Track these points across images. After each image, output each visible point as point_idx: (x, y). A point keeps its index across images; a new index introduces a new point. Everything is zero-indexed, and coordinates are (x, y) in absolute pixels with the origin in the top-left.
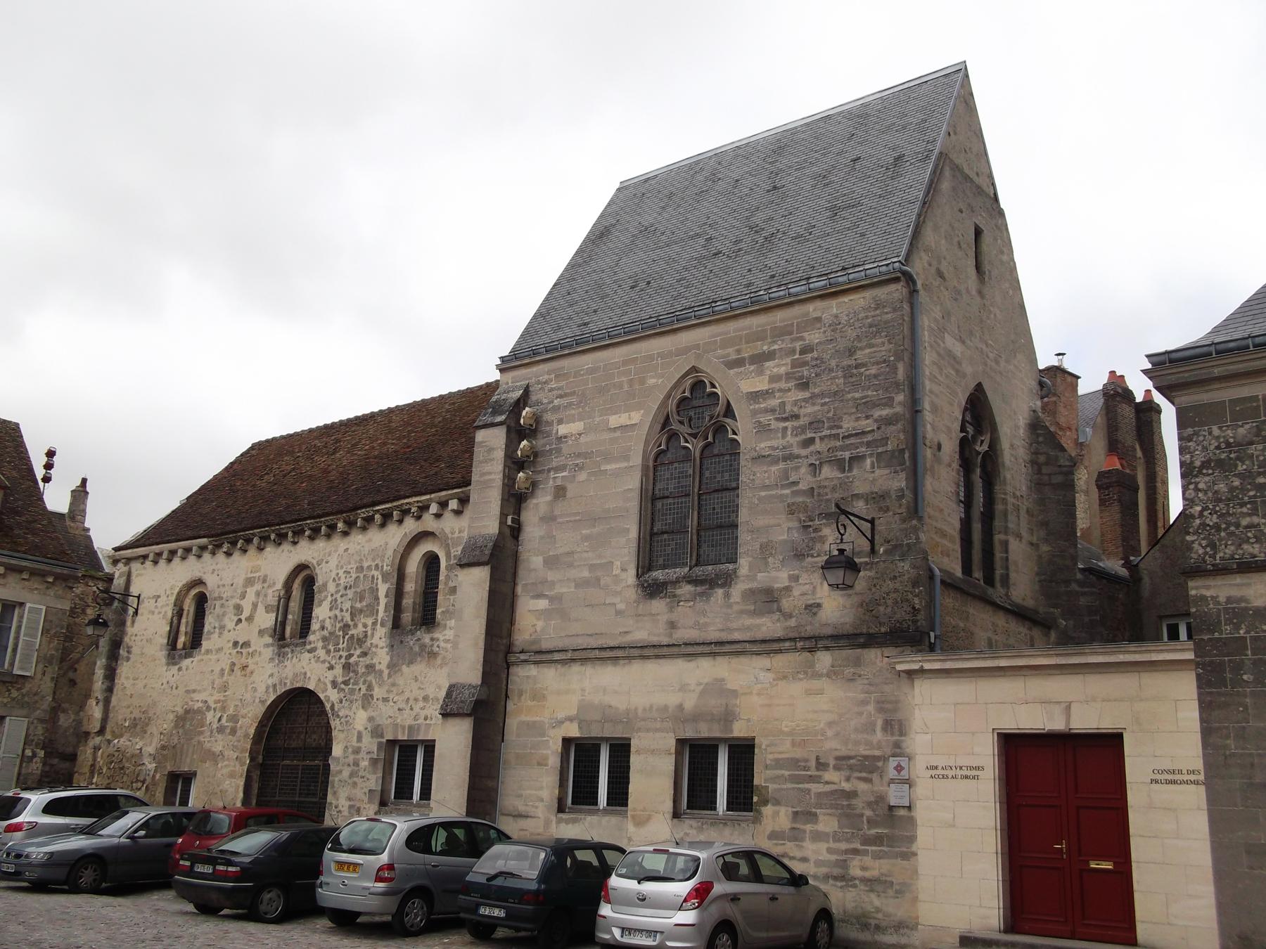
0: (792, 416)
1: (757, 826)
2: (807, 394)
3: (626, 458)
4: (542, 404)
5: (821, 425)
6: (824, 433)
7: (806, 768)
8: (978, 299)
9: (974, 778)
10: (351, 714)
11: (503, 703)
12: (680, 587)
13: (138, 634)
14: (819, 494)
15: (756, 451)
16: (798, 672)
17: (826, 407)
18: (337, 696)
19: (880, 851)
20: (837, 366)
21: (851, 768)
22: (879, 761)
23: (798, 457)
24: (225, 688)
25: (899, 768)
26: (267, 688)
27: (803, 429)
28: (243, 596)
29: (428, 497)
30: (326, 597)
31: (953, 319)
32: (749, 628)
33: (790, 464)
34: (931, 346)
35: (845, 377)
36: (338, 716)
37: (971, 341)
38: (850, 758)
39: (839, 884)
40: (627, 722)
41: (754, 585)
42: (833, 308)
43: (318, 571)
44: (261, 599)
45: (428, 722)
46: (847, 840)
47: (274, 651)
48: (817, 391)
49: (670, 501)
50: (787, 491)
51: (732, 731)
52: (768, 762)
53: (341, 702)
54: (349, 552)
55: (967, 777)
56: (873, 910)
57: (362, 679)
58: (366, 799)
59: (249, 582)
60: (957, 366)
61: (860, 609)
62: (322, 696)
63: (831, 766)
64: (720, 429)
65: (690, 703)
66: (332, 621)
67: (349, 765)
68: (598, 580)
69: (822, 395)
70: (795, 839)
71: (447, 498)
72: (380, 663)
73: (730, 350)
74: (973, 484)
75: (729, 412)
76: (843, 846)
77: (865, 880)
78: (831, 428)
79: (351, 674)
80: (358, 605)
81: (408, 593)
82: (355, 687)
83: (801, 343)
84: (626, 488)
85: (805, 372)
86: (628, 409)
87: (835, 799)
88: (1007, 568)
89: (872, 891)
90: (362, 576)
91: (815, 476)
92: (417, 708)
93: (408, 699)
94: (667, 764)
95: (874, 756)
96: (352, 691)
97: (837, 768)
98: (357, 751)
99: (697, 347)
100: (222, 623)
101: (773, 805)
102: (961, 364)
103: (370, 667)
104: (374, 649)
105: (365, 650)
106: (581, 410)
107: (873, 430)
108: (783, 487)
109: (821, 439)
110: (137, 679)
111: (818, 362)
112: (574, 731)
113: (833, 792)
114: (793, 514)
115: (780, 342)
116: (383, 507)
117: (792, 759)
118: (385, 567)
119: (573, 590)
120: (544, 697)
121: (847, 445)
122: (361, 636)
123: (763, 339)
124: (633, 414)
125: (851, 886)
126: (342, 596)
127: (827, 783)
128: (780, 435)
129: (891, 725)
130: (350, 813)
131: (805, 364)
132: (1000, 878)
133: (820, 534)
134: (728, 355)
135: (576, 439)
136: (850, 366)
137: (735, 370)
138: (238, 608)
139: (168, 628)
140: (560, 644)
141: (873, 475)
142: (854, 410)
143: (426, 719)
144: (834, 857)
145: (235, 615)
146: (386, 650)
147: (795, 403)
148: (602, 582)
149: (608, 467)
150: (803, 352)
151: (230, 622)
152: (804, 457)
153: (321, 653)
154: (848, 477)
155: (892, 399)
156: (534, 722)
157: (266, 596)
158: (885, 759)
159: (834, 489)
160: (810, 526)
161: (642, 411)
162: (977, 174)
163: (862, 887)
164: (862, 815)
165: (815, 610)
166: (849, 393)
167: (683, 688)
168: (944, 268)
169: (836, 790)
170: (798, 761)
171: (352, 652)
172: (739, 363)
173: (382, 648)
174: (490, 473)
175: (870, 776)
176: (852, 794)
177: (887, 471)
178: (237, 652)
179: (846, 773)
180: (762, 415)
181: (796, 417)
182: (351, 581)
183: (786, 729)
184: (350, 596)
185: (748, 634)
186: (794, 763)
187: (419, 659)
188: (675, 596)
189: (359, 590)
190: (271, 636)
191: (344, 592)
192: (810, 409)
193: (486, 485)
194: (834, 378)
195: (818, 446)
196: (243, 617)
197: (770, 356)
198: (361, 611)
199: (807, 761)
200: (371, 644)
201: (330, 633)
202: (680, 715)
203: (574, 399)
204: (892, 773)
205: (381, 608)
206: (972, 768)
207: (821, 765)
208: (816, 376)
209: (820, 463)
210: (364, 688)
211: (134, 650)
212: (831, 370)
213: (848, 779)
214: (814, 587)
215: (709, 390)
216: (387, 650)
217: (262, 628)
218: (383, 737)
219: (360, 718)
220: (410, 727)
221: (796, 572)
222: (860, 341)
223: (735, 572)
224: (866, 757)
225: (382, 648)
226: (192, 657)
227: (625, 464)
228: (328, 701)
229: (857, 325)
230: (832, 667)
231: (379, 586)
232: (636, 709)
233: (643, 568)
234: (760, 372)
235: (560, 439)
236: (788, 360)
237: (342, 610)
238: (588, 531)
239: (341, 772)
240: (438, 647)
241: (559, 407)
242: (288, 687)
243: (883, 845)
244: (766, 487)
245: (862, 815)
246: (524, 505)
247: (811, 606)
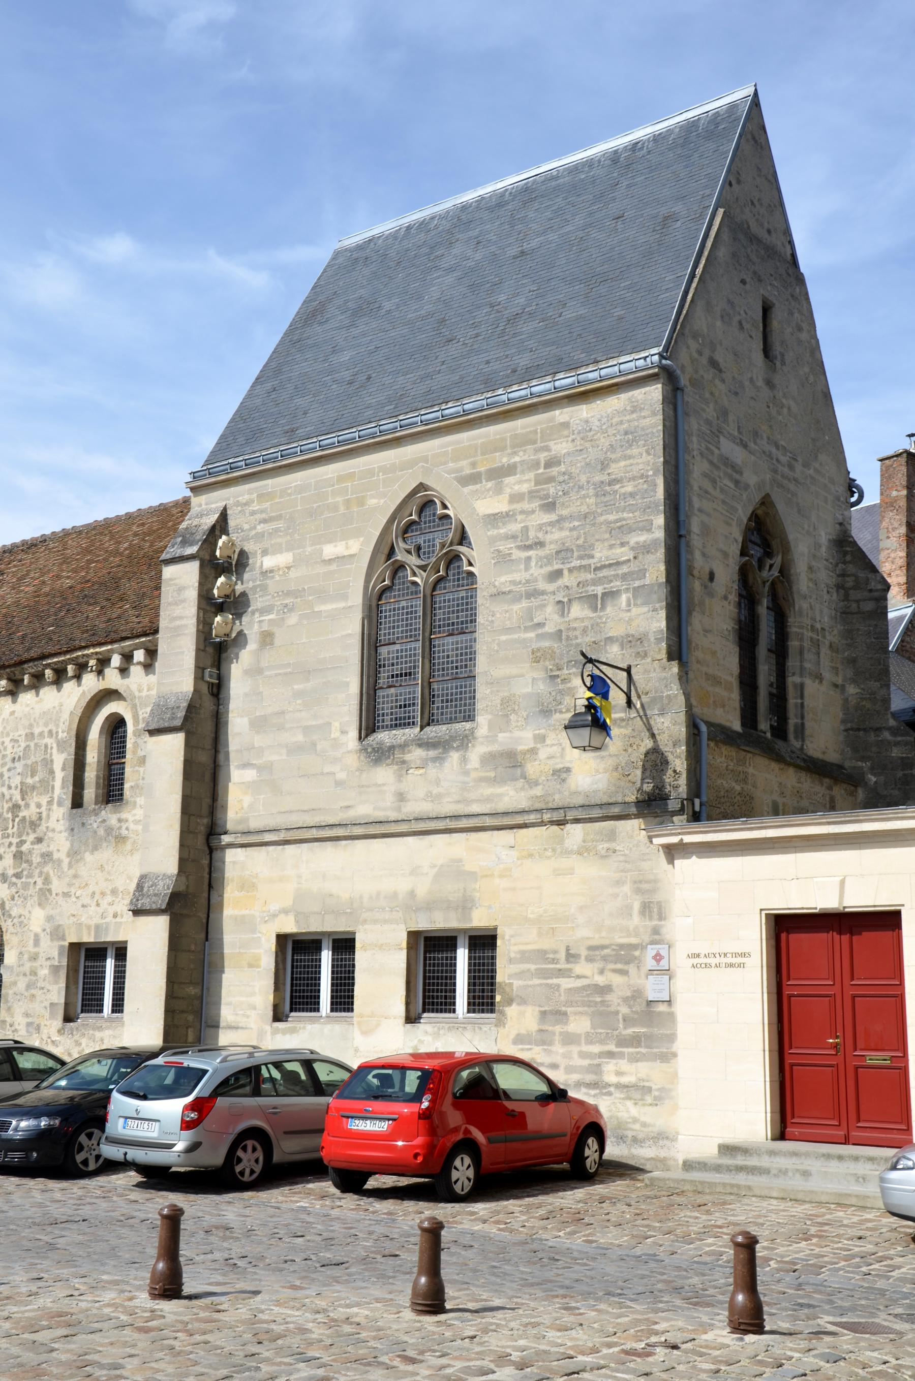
0: (536, 544)
1: (501, 1030)
2: (553, 517)
3: (344, 597)
4: (242, 531)
5: (569, 555)
6: (573, 565)
7: (554, 961)
8: (766, 392)
9: (739, 966)
10: (26, 913)
11: (205, 895)
12: (409, 752)
14: (568, 638)
15: (495, 587)
16: (545, 849)
17: (575, 533)
18: (8, 892)
19: (637, 1053)
20: (588, 482)
21: (605, 959)
22: (636, 950)
23: (543, 593)
25: (658, 958)
27: (549, 559)
29: (109, 647)
31: (731, 418)
32: (488, 799)
33: (535, 602)
34: (701, 454)
35: (597, 495)
36: (10, 916)
37: (755, 443)
38: (603, 947)
40: (351, 913)
41: (495, 748)
42: (584, 411)
45: (118, 919)
46: (602, 1042)
48: (565, 512)
49: (397, 647)
50: (532, 635)
51: (471, 920)
52: (512, 955)
53: (13, 899)
54: (16, 715)
55: (731, 965)
56: (629, 1120)
57: (38, 871)
58: (47, 1015)
60: (737, 477)
61: (615, 774)
63: (583, 958)
64: (453, 559)
65: (423, 888)
67: (25, 975)
68: (314, 744)
69: (571, 517)
70: (543, 1043)
71: (131, 648)
73: (464, 463)
74: (758, 617)
75: (463, 538)
76: (596, 1049)
77: (618, 1086)
78: (581, 558)
79: (24, 865)
80: (29, 781)
81: (90, 765)
82: (28, 880)
83: (546, 454)
84: (344, 633)
85: (552, 489)
86: (345, 536)
87: (588, 995)
88: (803, 717)
90: (32, 744)
91: (563, 615)
92: (104, 903)
93: (94, 893)
94: (398, 960)
96: (26, 886)
97: (590, 959)
98: (34, 958)
99: (425, 459)
101: (519, 1004)
102: (741, 473)
103: (47, 856)
104: (50, 834)
105: (41, 835)
106: (289, 537)
107: (629, 561)
108: (526, 629)
109: (570, 570)
111: (566, 477)
112: (290, 927)
113: (584, 988)
114: (539, 662)
115: (521, 453)
116: (55, 660)
117: (538, 951)
118: (60, 735)
119: (284, 757)
120: (253, 886)
121: (600, 578)
123: (503, 449)
124: (351, 542)
125: (606, 1094)
126: (9, 770)
127: (578, 977)
128: (522, 567)
129: (649, 907)
130: (28, 1031)
131: (551, 480)
132: (768, 1079)
133: (569, 685)
134: (461, 469)
135: (284, 573)
136: (602, 482)
137: (470, 487)
140: (271, 823)
141: (629, 614)
142: (607, 536)
143: (115, 916)
144: (586, 1062)
146: (66, 834)
147: (540, 527)
148: (319, 747)
149: (323, 608)
150: (549, 464)
152: (550, 593)
154: (600, 618)
155: (651, 523)
156: (243, 916)
158: (642, 947)
159: (585, 631)
160: (558, 676)
161: (362, 539)
162: (769, 232)
164: (617, 1013)
165: (564, 775)
166: (602, 515)
167: (415, 871)
168: (719, 357)
169: (589, 985)
170: (544, 952)
171: (24, 838)
172: (474, 479)
173: (61, 832)
174: (181, 618)
175: (625, 967)
176: (606, 989)
177: (645, 609)
179: (599, 965)
180: (502, 542)
181: (540, 544)
182: (19, 751)
183: (531, 916)
184: (19, 770)
185: (488, 806)
186: (542, 955)
187: (105, 844)
188: (404, 762)
189: (29, 762)
191: (12, 765)
192: (556, 535)
193: (177, 632)
194: (585, 497)
195: (567, 579)
197: (510, 470)
198: (33, 788)
199: (555, 952)
202: (411, 903)
203: (280, 524)
204: (650, 963)
205: (58, 783)
206: (736, 955)
207: (571, 957)
208: (564, 494)
209: (570, 600)
210: (40, 882)
212: (581, 488)
213: (602, 972)
214: (563, 749)
215: (440, 511)
218: (64, 939)
219: (37, 918)
220: (98, 927)
221: (542, 731)
222: (614, 452)
223: (473, 732)
224: (622, 946)
225: (61, 832)
227: (342, 605)
229: (611, 431)
230: (584, 841)
231: (54, 757)
232: (361, 897)
233: (367, 729)
234: (499, 490)
235: (265, 573)
236: (531, 475)
237: (10, 787)
238: (301, 686)
239: (15, 983)
240: (127, 829)
241: (262, 535)
244: (508, 630)
245: (617, 1013)
246: (224, 655)
247: (560, 771)
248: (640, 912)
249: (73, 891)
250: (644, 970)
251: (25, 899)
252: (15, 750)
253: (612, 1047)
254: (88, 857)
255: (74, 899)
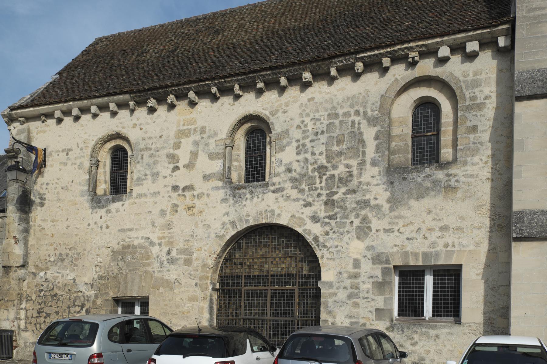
13: (50, 183)
24: (169, 226)
26: (224, 224)
28: (177, 145)
30: (289, 143)
43: (272, 120)
44: (201, 148)
45: (449, 249)
47: (226, 192)
57: (354, 214)
59: (183, 133)
62: (300, 230)
66: (302, 164)
72: (376, 199)
79: (336, 210)
80: (335, 148)
82: (344, 221)
93: (419, 229)
100: (155, 171)
103: (364, 204)
110: (57, 221)
122: (343, 176)
126: (311, 141)
138: (173, 158)
139: (88, 177)
145: (169, 163)
151: (164, 168)
153: (294, 193)
157: (207, 145)
178: (179, 195)
187: (433, 193)
189: (335, 135)
190: (220, 180)
191: (315, 138)
196: (180, 164)
198: (340, 153)
200: (360, 183)
201: (300, 174)
211: (47, 196)
216: (382, 186)
217: (208, 172)
226: (122, 200)
228: (309, 233)
237: (313, 154)
242: (252, 223)
249: (396, 228)
251: (342, 234)
252: (317, 126)
254: (412, 202)
255: (398, 234)
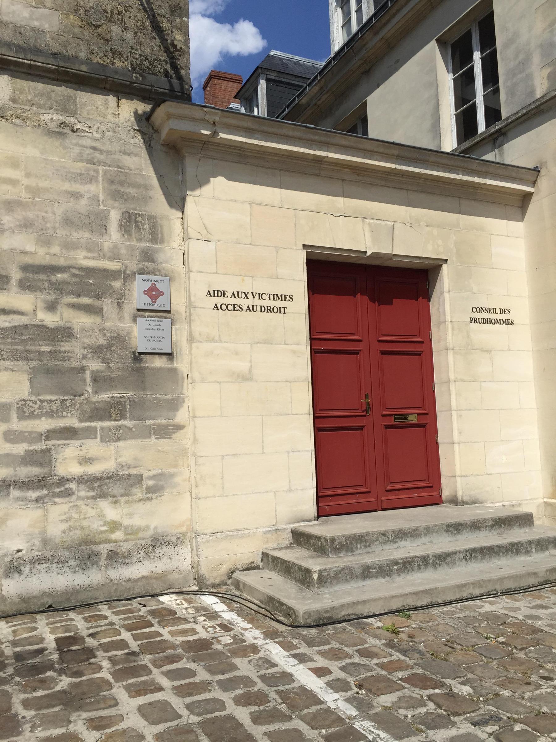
9: (279, 310)
19: (118, 428)
22: (115, 280)
38: (54, 269)
39: (33, 494)
46: (51, 414)
55: (269, 310)
56: (104, 528)
87: (23, 342)
89: (103, 496)
95: (106, 270)
113: (15, 330)
125: (60, 495)
129: (136, 222)
144: (20, 449)
163: (83, 494)
164: (82, 369)
175: (98, 303)
213: (51, 307)
224: (89, 271)
243: (123, 417)
245: (82, 369)
248: (121, 226)
250: (129, 309)
253: (72, 421)
